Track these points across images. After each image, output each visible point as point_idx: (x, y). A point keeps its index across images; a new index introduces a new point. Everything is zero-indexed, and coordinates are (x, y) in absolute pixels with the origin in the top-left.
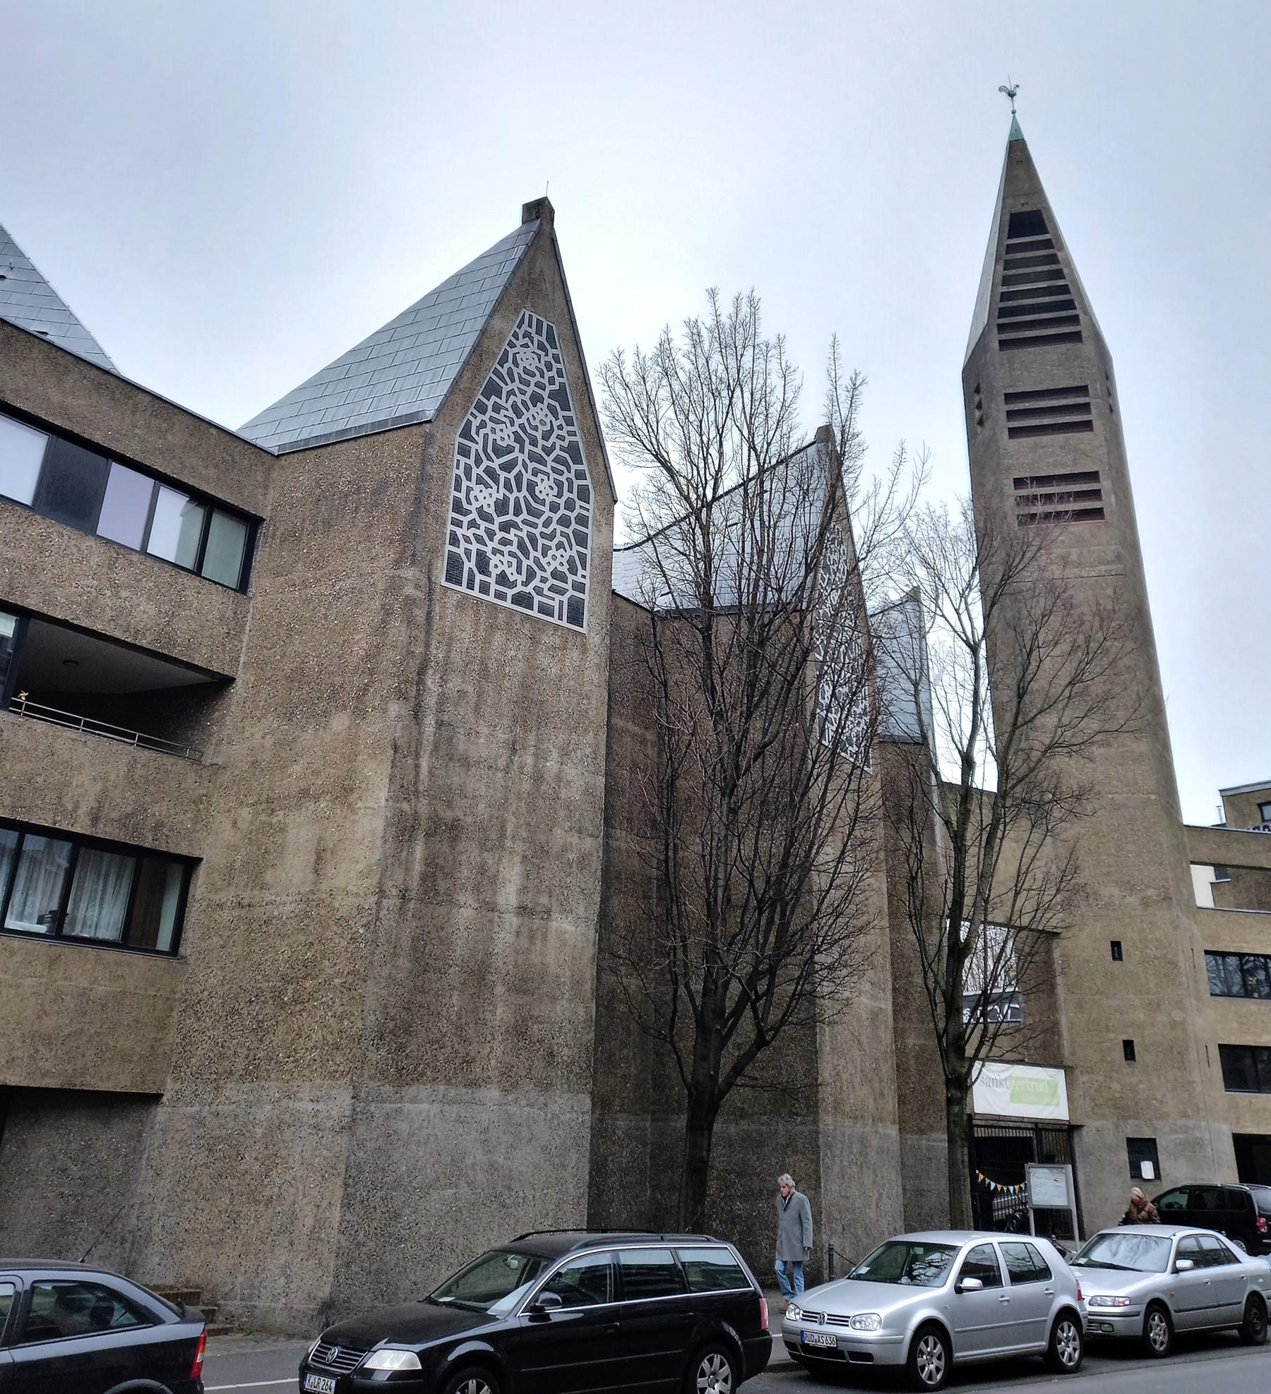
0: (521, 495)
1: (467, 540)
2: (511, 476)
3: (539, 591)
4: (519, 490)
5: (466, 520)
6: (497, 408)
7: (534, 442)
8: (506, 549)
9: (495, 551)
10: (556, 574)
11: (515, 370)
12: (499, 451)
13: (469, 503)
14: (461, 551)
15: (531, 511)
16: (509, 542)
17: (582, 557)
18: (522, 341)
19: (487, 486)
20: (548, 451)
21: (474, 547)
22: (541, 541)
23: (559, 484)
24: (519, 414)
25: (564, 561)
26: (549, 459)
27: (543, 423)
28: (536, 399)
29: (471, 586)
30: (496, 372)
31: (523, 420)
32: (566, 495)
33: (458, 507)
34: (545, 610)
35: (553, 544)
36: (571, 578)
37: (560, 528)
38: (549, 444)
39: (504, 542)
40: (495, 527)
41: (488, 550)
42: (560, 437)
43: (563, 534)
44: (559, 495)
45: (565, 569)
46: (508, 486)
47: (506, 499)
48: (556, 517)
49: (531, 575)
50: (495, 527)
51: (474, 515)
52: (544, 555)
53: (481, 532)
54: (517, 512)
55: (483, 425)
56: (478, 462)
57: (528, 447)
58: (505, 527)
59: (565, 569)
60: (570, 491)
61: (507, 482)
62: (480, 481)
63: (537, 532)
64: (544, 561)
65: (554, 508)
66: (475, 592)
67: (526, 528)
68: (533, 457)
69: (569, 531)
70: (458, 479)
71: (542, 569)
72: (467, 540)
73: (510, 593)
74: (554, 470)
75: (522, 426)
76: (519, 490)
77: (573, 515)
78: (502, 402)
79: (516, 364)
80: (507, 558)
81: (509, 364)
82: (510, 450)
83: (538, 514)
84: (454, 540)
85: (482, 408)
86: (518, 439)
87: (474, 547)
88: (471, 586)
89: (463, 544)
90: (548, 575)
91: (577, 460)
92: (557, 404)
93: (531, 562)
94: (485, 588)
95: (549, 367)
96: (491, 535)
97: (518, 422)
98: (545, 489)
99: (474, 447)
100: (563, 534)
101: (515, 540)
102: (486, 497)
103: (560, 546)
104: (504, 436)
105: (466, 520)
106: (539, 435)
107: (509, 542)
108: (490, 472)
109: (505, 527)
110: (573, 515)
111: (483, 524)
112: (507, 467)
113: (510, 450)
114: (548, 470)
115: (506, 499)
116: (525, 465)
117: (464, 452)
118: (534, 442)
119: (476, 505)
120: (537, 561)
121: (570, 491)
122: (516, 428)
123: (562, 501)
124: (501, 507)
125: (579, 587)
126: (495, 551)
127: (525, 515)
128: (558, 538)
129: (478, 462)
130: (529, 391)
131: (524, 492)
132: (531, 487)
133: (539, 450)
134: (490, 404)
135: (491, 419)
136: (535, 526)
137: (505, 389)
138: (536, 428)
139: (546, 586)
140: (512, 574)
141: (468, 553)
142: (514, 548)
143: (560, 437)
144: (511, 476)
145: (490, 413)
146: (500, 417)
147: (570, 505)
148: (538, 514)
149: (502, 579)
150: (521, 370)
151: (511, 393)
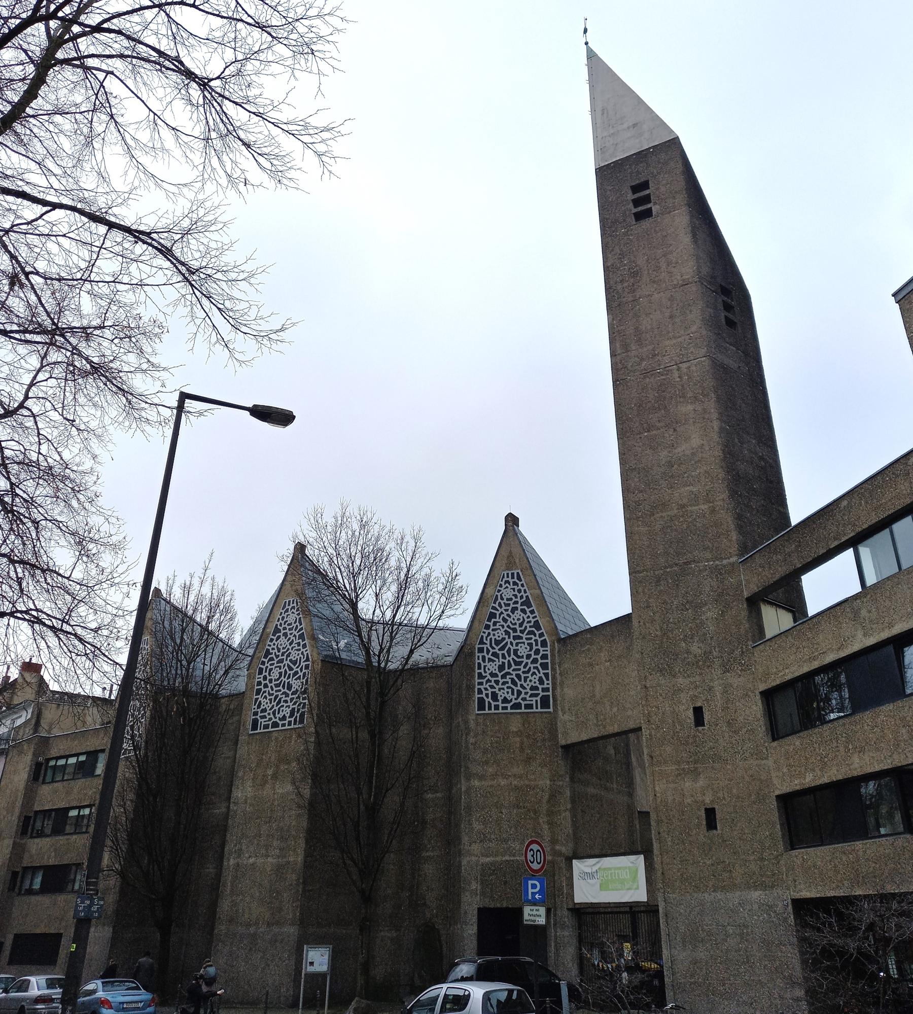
0: (510, 659)
1: (486, 689)
2: (505, 652)
3: (524, 699)
4: (509, 656)
5: (484, 681)
8: (505, 687)
9: (500, 689)
10: (532, 688)
11: (502, 602)
12: (497, 642)
13: (485, 672)
14: (484, 696)
15: (516, 663)
16: (507, 682)
17: (546, 675)
18: (504, 586)
19: (494, 661)
20: (522, 632)
21: (490, 690)
22: (523, 676)
23: (530, 645)
24: (505, 620)
25: (536, 680)
27: (518, 619)
28: (514, 610)
29: (490, 709)
30: (493, 608)
31: (509, 623)
32: (535, 648)
35: (529, 675)
36: (540, 687)
37: (532, 666)
38: (523, 628)
39: (504, 683)
40: (499, 678)
41: (497, 690)
42: (529, 622)
43: (534, 668)
44: (531, 650)
45: (537, 684)
47: (503, 663)
48: (529, 661)
50: (499, 678)
51: (489, 677)
52: (525, 681)
53: (493, 683)
55: (489, 634)
56: (488, 651)
57: (512, 634)
58: (504, 677)
59: (537, 684)
60: (537, 645)
61: (503, 654)
62: (490, 660)
63: (520, 672)
64: (525, 685)
66: (493, 711)
67: (514, 673)
68: (515, 638)
69: (538, 665)
70: (479, 664)
71: (524, 688)
72: (486, 689)
73: (509, 705)
74: (527, 639)
75: (508, 626)
76: (509, 656)
77: (539, 657)
78: (497, 620)
79: (502, 599)
80: (506, 690)
81: (499, 600)
82: (504, 639)
83: (520, 663)
85: (487, 627)
87: (490, 690)
88: (490, 709)
89: (484, 692)
90: (528, 690)
91: (539, 628)
92: (525, 607)
93: (519, 688)
95: (519, 591)
96: (497, 682)
97: (505, 625)
98: (523, 650)
99: (485, 646)
100: (534, 668)
101: (510, 681)
102: (493, 667)
103: (534, 673)
104: (500, 634)
105: (484, 681)
106: (517, 626)
107: (507, 682)
108: (495, 654)
109: (504, 677)
110: (539, 657)
111: (493, 679)
112: (502, 649)
113: (504, 639)
114: (524, 640)
115: (503, 663)
116: (511, 643)
118: (515, 630)
119: (488, 672)
120: (522, 686)
121: (537, 645)
122: (506, 628)
123: (532, 653)
124: (501, 668)
125: (547, 690)
126: (500, 689)
127: (514, 667)
128: (532, 670)
129: (488, 651)
130: (510, 608)
131: (512, 656)
133: (518, 633)
134: (491, 624)
135: (493, 630)
136: (519, 670)
137: (498, 613)
138: (515, 624)
139: (527, 697)
140: (509, 696)
141: (487, 695)
142: (510, 684)
143: (529, 622)
144: (505, 652)
145: (492, 627)
146: (497, 627)
147: (537, 652)
148: (520, 663)
149: (505, 700)
150: (505, 601)
151: (502, 613)
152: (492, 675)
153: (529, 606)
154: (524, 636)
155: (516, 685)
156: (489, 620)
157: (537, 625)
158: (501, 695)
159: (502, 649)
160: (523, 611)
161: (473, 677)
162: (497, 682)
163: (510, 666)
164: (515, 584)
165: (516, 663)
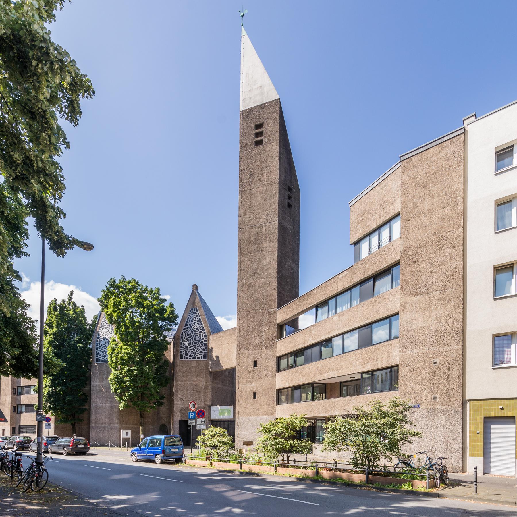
6: (187, 328)
7: (195, 331)
10: (200, 352)
12: (188, 335)
17: (206, 348)
21: (185, 352)
26: (198, 333)
28: (195, 323)
33: (181, 347)
34: (199, 358)
46: (190, 340)
49: (196, 353)
54: (192, 344)
58: (190, 347)
65: (199, 341)
68: (195, 334)
84: (181, 352)
85: (184, 329)
86: (192, 332)
91: (204, 330)
94: (187, 358)
96: (188, 349)
112: (190, 337)
117: (182, 338)
124: (189, 344)
125: (206, 353)
132: (195, 339)
140: (192, 354)
149: (190, 356)
152: (186, 347)
153: (201, 322)
154: (198, 333)
155: (194, 350)
156: (185, 326)
157: (203, 329)
158: (189, 354)
159: (190, 337)
160: (198, 324)
161: (179, 347)
162: (188, 349)
163: (192, 344)
164: (195, 313)
165: (195, 343)
